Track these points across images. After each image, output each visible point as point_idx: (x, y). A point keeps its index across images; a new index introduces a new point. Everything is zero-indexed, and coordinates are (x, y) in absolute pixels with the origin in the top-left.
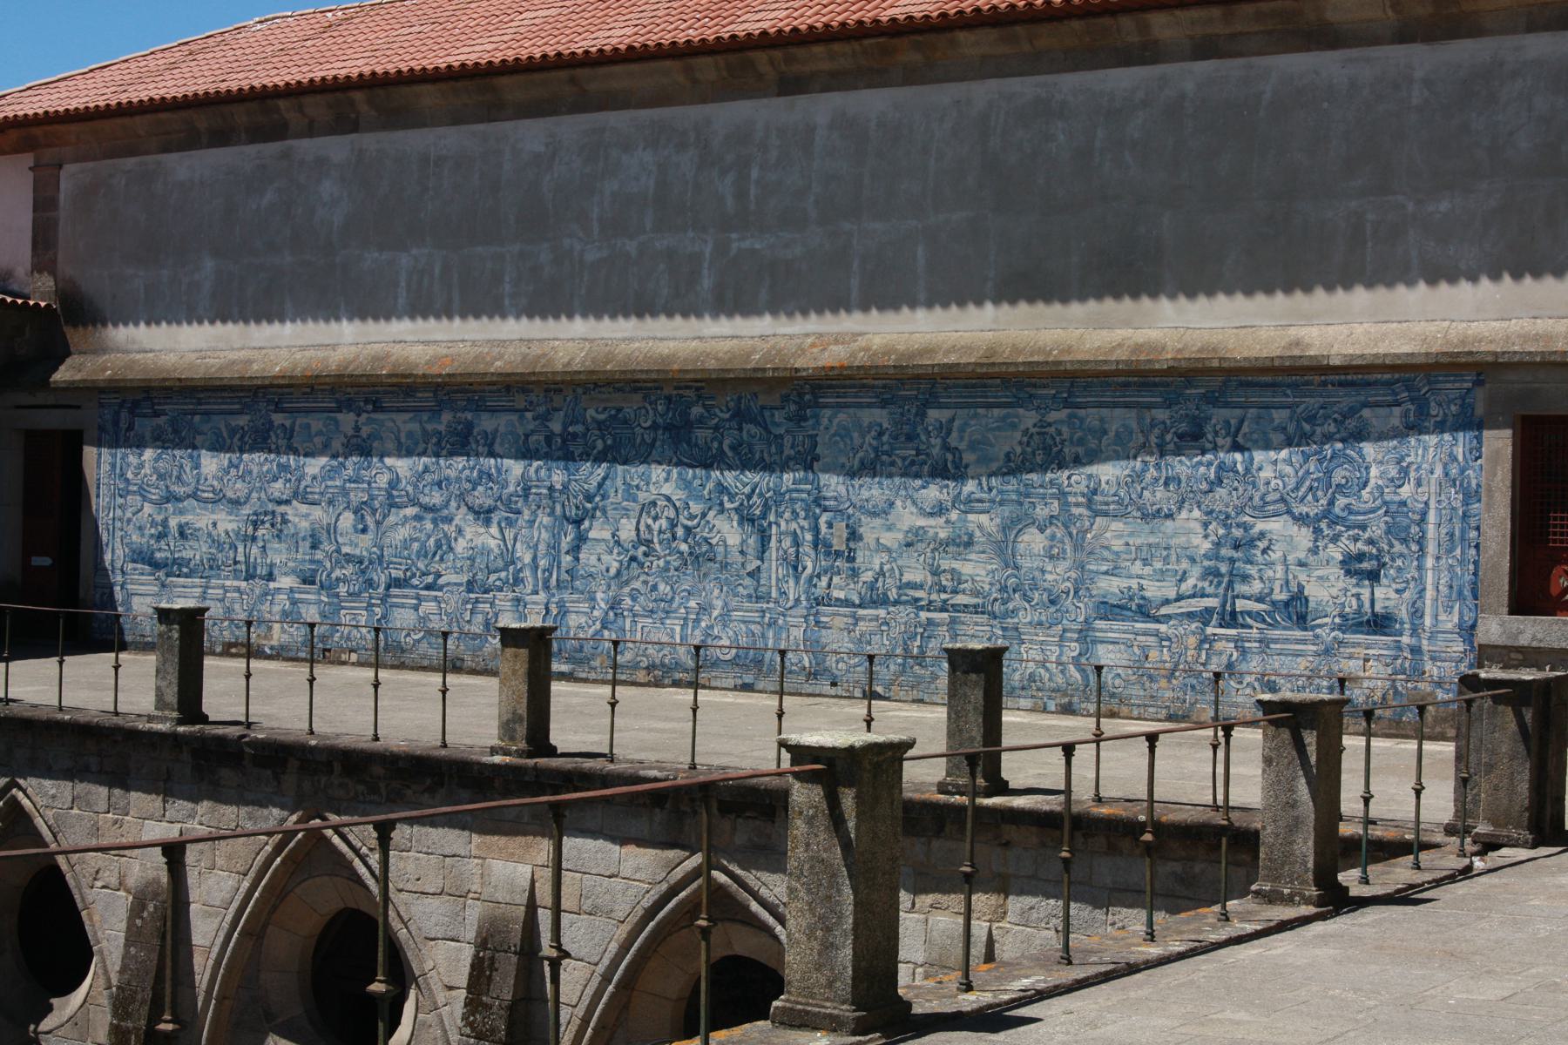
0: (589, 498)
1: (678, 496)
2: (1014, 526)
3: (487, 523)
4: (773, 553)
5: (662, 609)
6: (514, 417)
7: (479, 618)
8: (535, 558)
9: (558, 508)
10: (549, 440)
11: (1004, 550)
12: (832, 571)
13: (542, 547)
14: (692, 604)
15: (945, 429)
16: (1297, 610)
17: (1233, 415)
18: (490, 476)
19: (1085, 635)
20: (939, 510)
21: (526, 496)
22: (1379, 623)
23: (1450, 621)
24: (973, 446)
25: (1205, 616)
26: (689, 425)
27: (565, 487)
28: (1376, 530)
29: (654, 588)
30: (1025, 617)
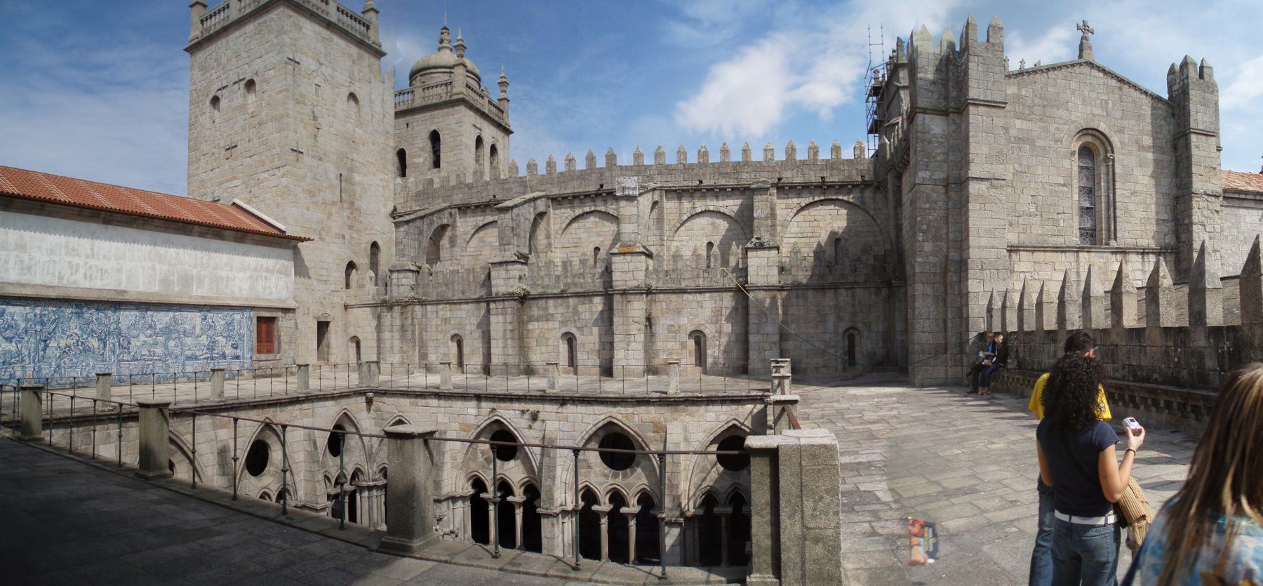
0: (49, 334)
1: (79, 333)
2: (167, 340)
3: (11, 342)
4: (107, 348)
5: (74, 366)
6: (22, 308)
7: (8, 374)
8: (29, 353)
9: (38, 338)
10: (35, 315)
11: (166, 348)
12: (123, 353)
13: (32, 349)
14: (84, 364)
15: (152, 316)
16: (224, 356)
17: (212, 315)
18: (12, 327)
19: (183, 365)
20: (150, 336)
21: (26, 334)
22: (238, 357)
23: (248, 356)
24: (158, 320)
25: (207, 358)
26: (83, 313)
27: (41, 331)
28: (236, 339)
29: (72, 360)
30: (170, 361)
